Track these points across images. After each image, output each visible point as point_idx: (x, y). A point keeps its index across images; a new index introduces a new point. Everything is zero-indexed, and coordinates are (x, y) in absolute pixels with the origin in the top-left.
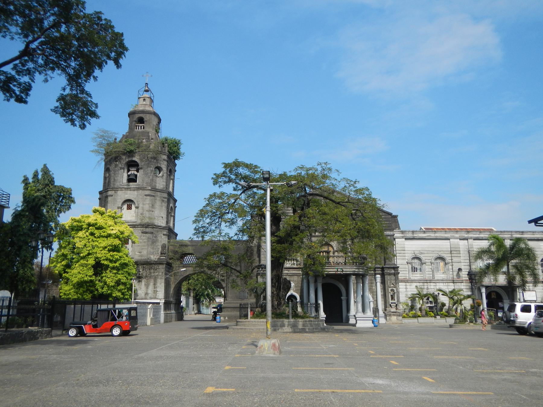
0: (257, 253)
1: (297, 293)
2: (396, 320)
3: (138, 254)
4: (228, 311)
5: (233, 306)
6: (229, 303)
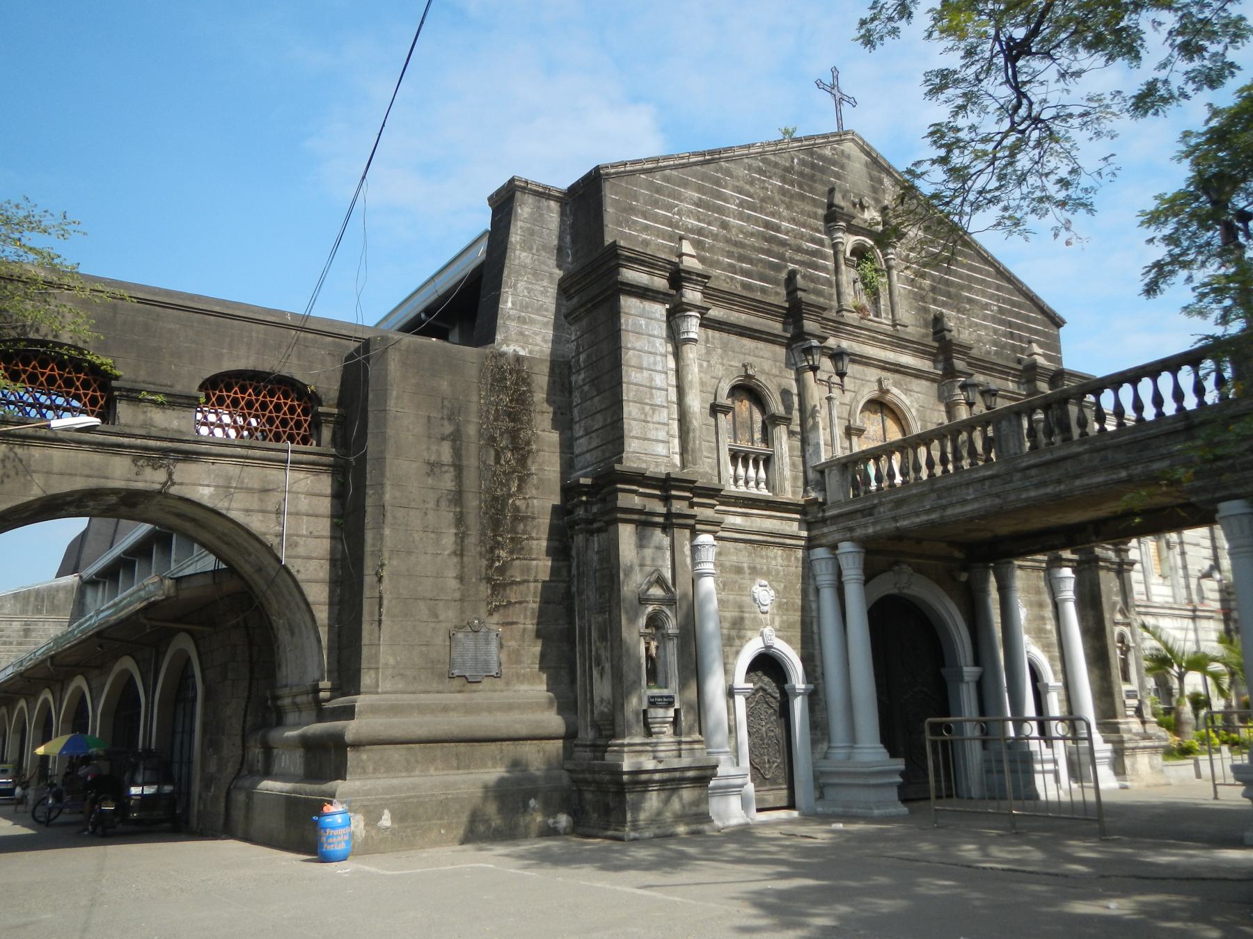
0: (549, 401)
1: (788, 641)
2: (1149, 770)
4: (390, 769)
5: (421, 732)
6: (395, 710)
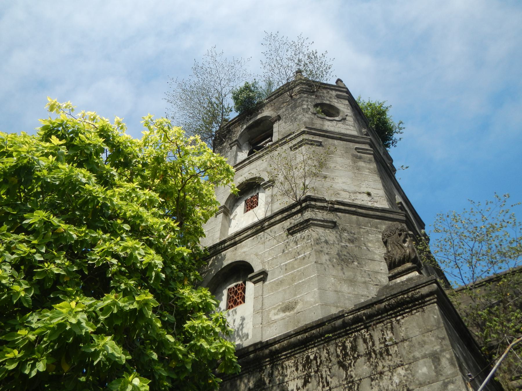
3: (282, 315)
